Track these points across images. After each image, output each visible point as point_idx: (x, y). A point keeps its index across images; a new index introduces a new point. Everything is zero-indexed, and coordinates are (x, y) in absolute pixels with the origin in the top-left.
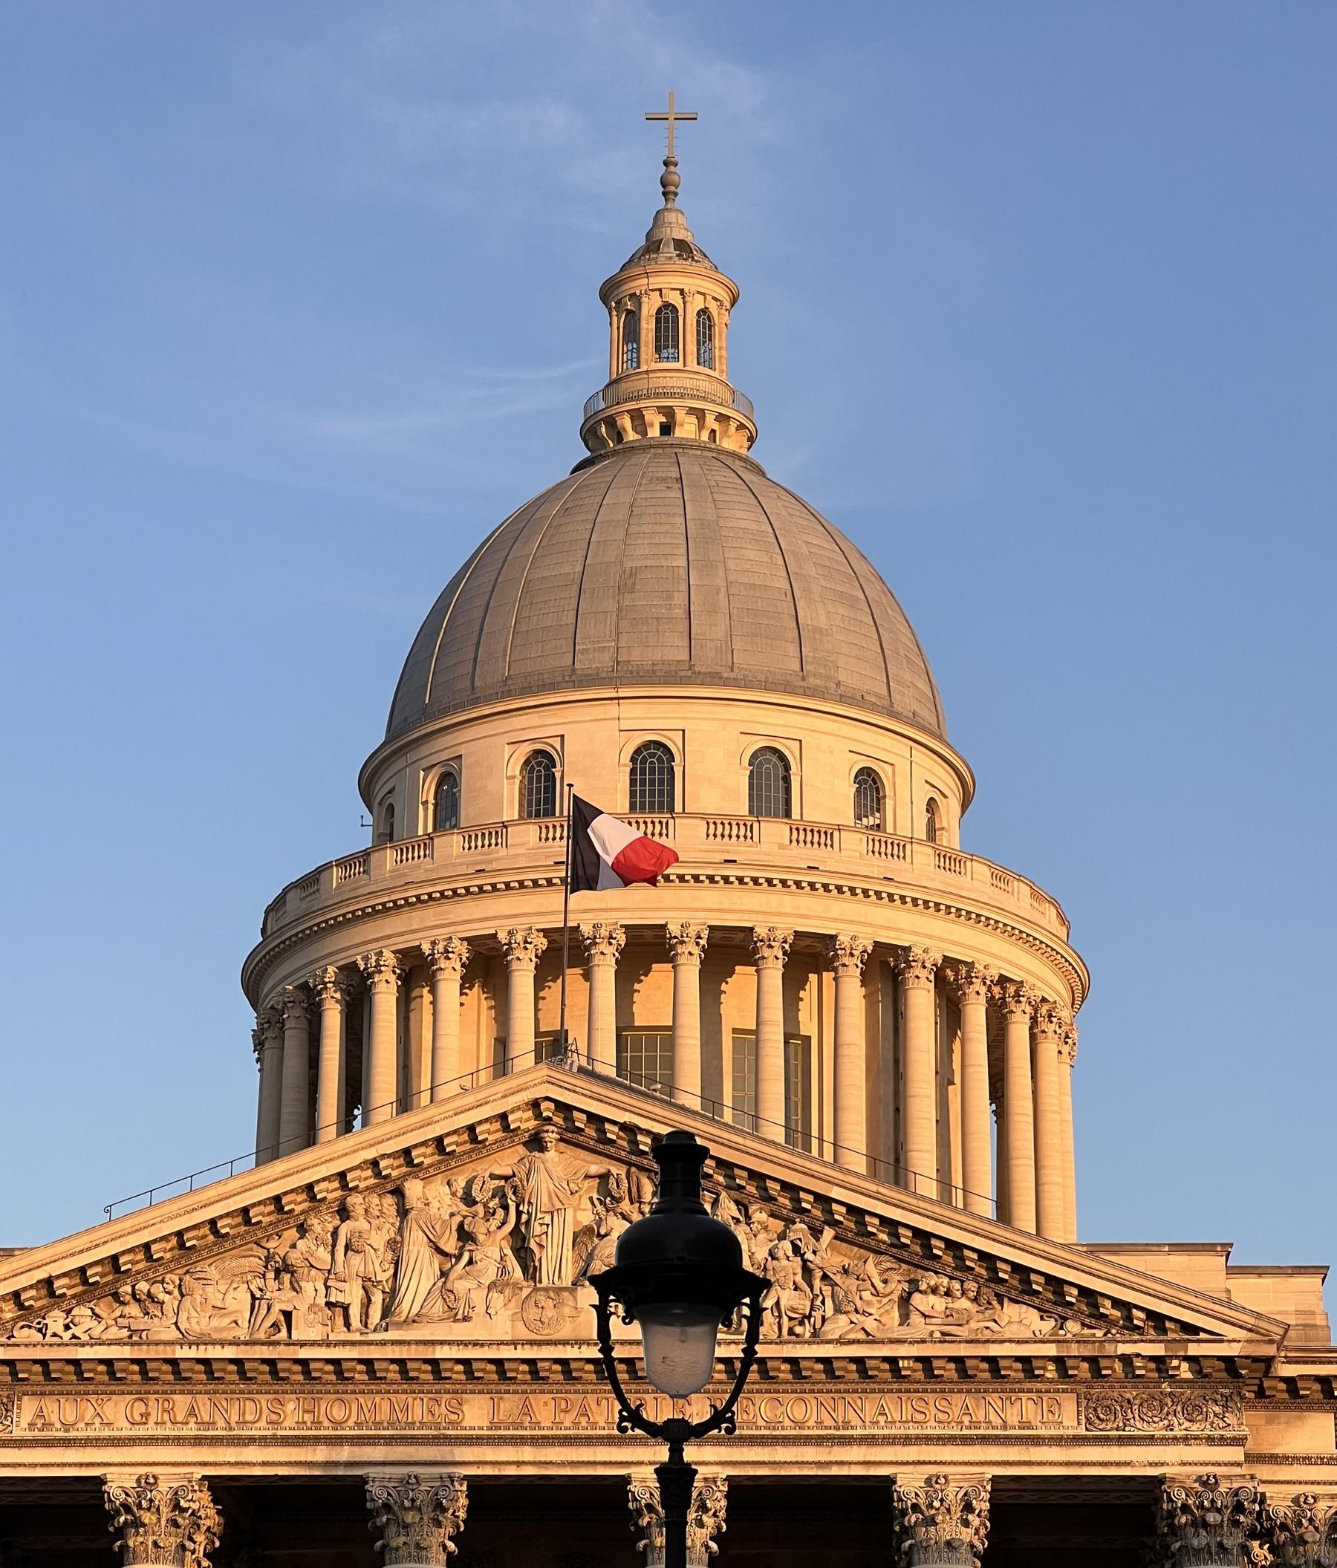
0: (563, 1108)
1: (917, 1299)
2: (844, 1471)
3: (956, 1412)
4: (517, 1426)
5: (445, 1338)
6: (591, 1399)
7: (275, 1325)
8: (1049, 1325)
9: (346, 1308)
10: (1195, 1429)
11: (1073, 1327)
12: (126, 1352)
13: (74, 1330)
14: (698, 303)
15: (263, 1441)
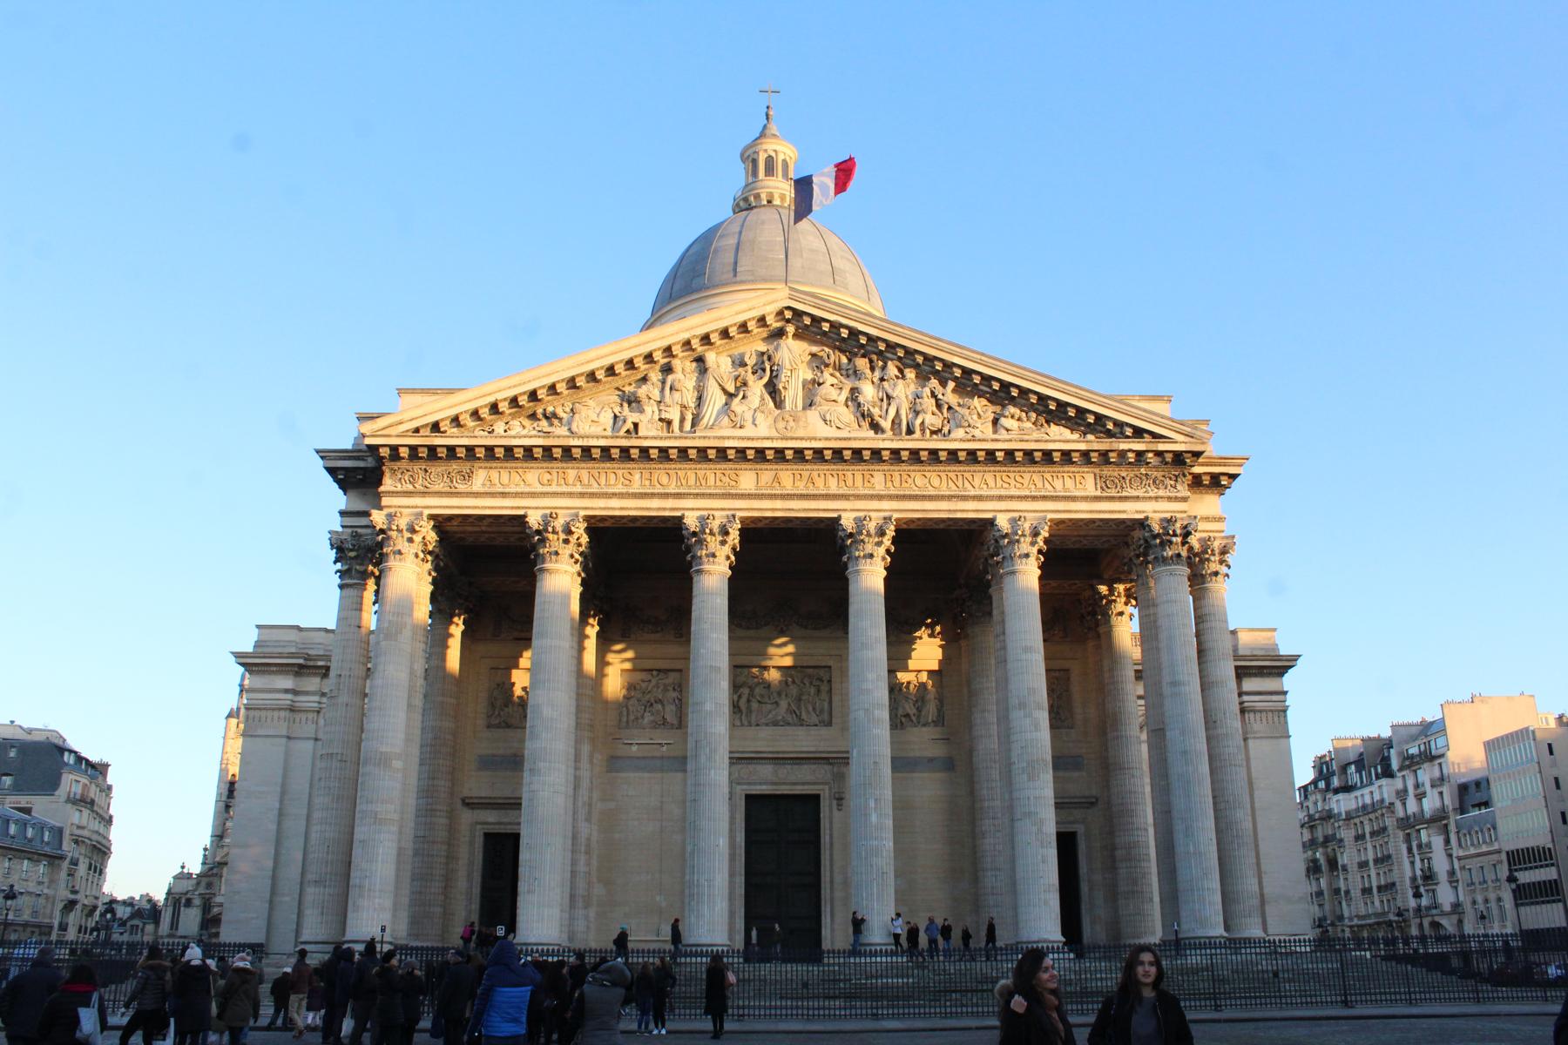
0: (798, 314)
1: (1003, 421)
2: (964, 515)
3: (1026, 482)
4: (772, 487)
5: (731, 438)
6: (815, 474)
7: (628, 431)
8: (1076, 436)
9: (669, 423)
10: (1161, 493)
11: (1090, 437)
12: (540, 442)
13: (512, 433)
14: (781, 157)
15: (621, 496)
